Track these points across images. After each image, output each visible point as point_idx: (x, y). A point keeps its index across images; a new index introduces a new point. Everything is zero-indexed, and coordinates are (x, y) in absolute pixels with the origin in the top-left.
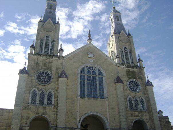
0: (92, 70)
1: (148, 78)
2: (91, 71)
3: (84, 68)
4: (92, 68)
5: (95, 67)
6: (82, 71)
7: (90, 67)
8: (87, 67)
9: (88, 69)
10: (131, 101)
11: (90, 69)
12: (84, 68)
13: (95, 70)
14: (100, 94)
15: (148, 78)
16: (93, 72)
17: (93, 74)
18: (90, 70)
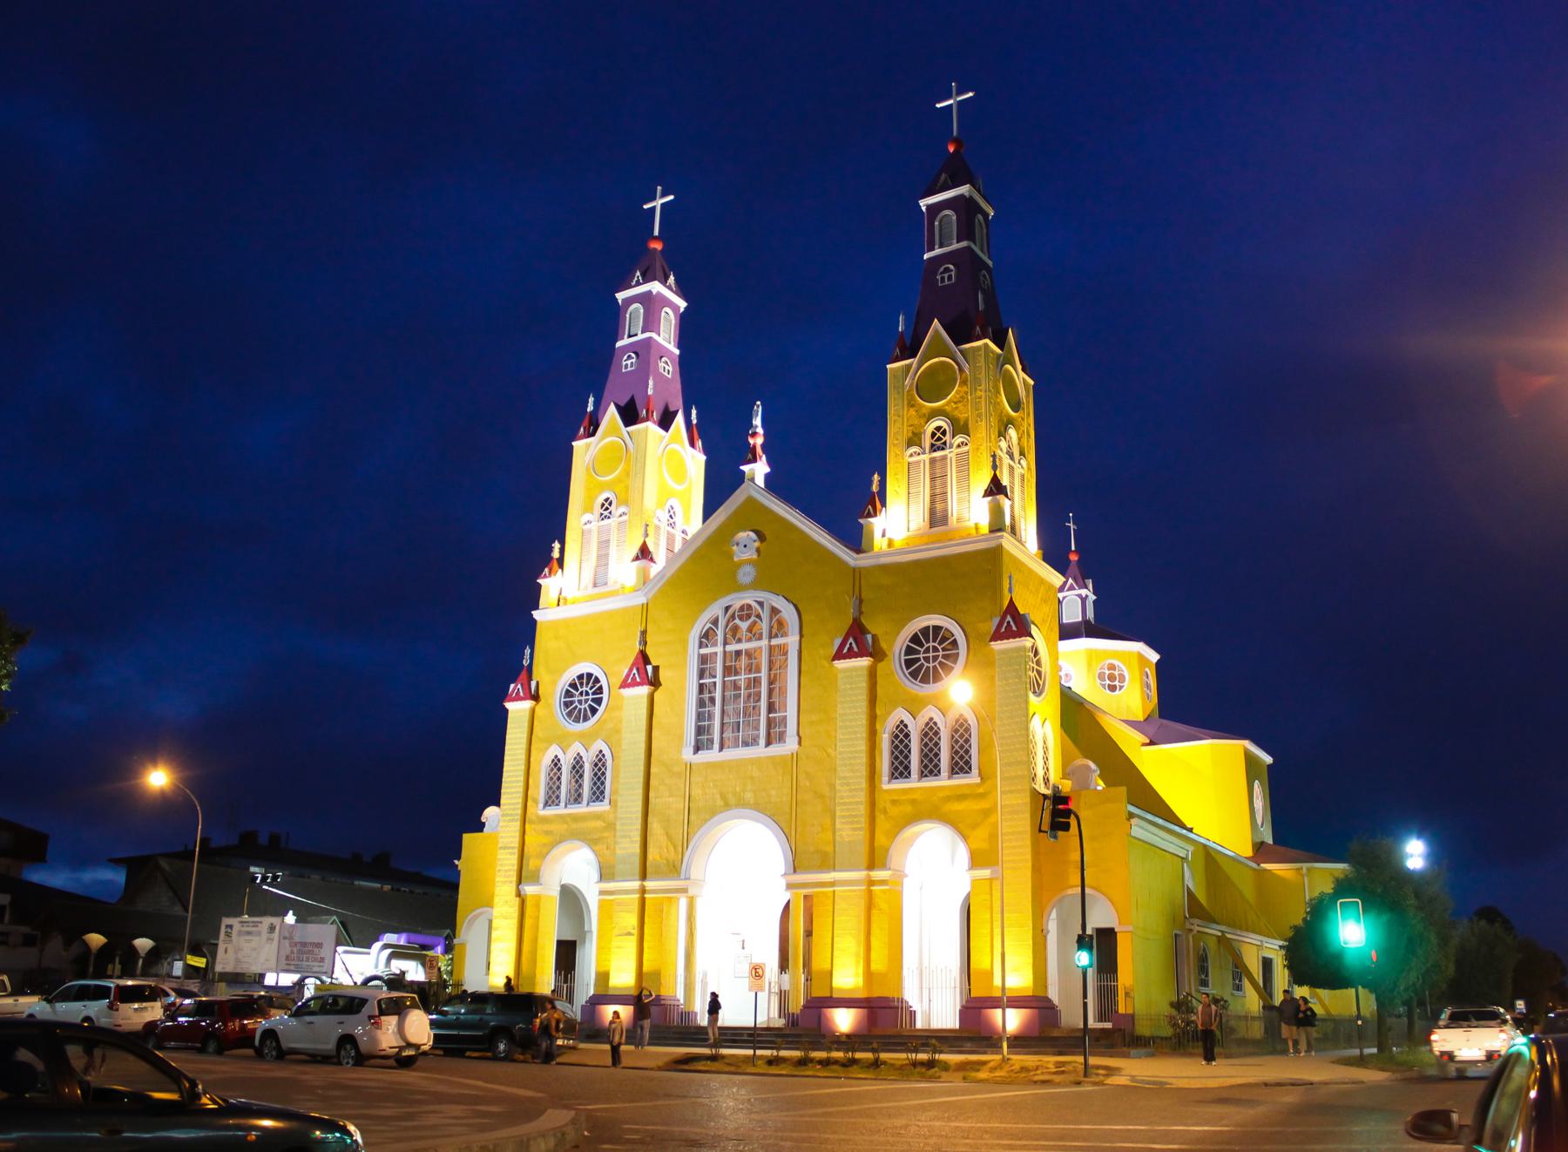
0: (749, 616)
1: (1010, 590)
2: (744, 625)
3: (715, 622)
4: (749, 607)
5: (761, 604)
6: (707, 637)
7: (742, 609)
8: (727, 609)
9: (733, 617)
10: (907, 735)
11: (741, 618)
12: (715, 622)
13: (758, 616)
14: (770, 723)
15: (1010, 590)
16: (750, 630)
17: (749, 640)
18: (737, 621)
